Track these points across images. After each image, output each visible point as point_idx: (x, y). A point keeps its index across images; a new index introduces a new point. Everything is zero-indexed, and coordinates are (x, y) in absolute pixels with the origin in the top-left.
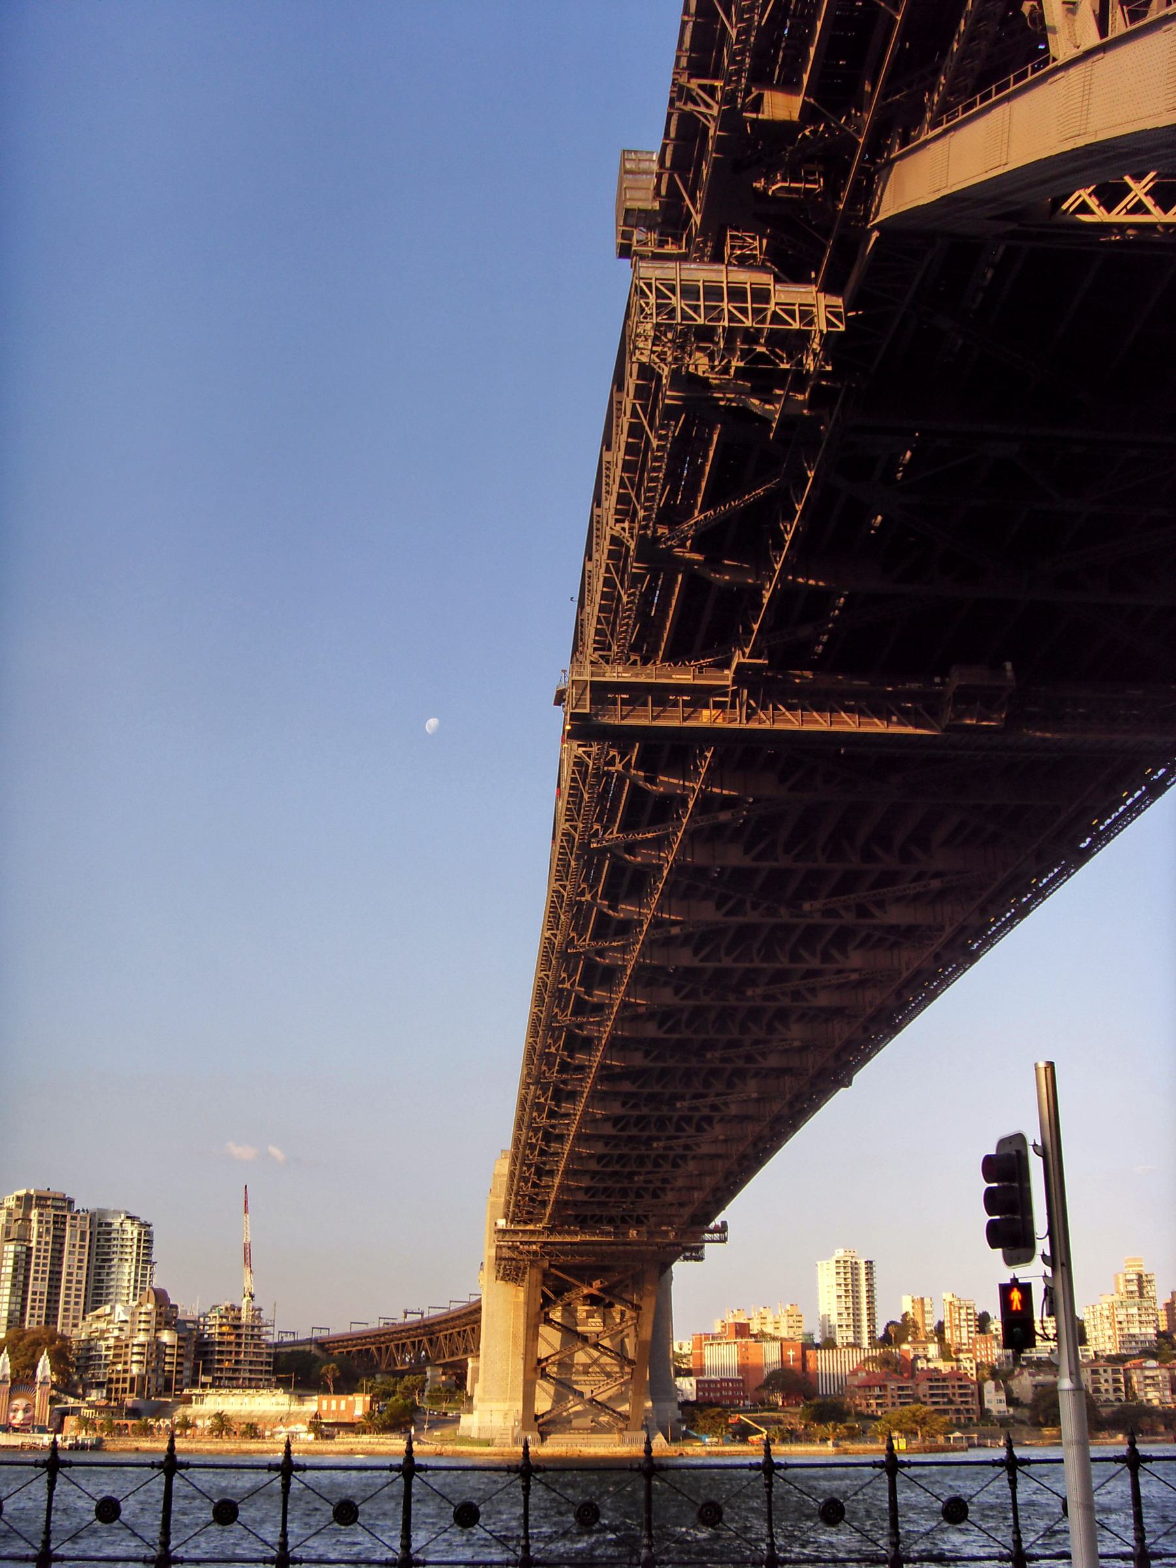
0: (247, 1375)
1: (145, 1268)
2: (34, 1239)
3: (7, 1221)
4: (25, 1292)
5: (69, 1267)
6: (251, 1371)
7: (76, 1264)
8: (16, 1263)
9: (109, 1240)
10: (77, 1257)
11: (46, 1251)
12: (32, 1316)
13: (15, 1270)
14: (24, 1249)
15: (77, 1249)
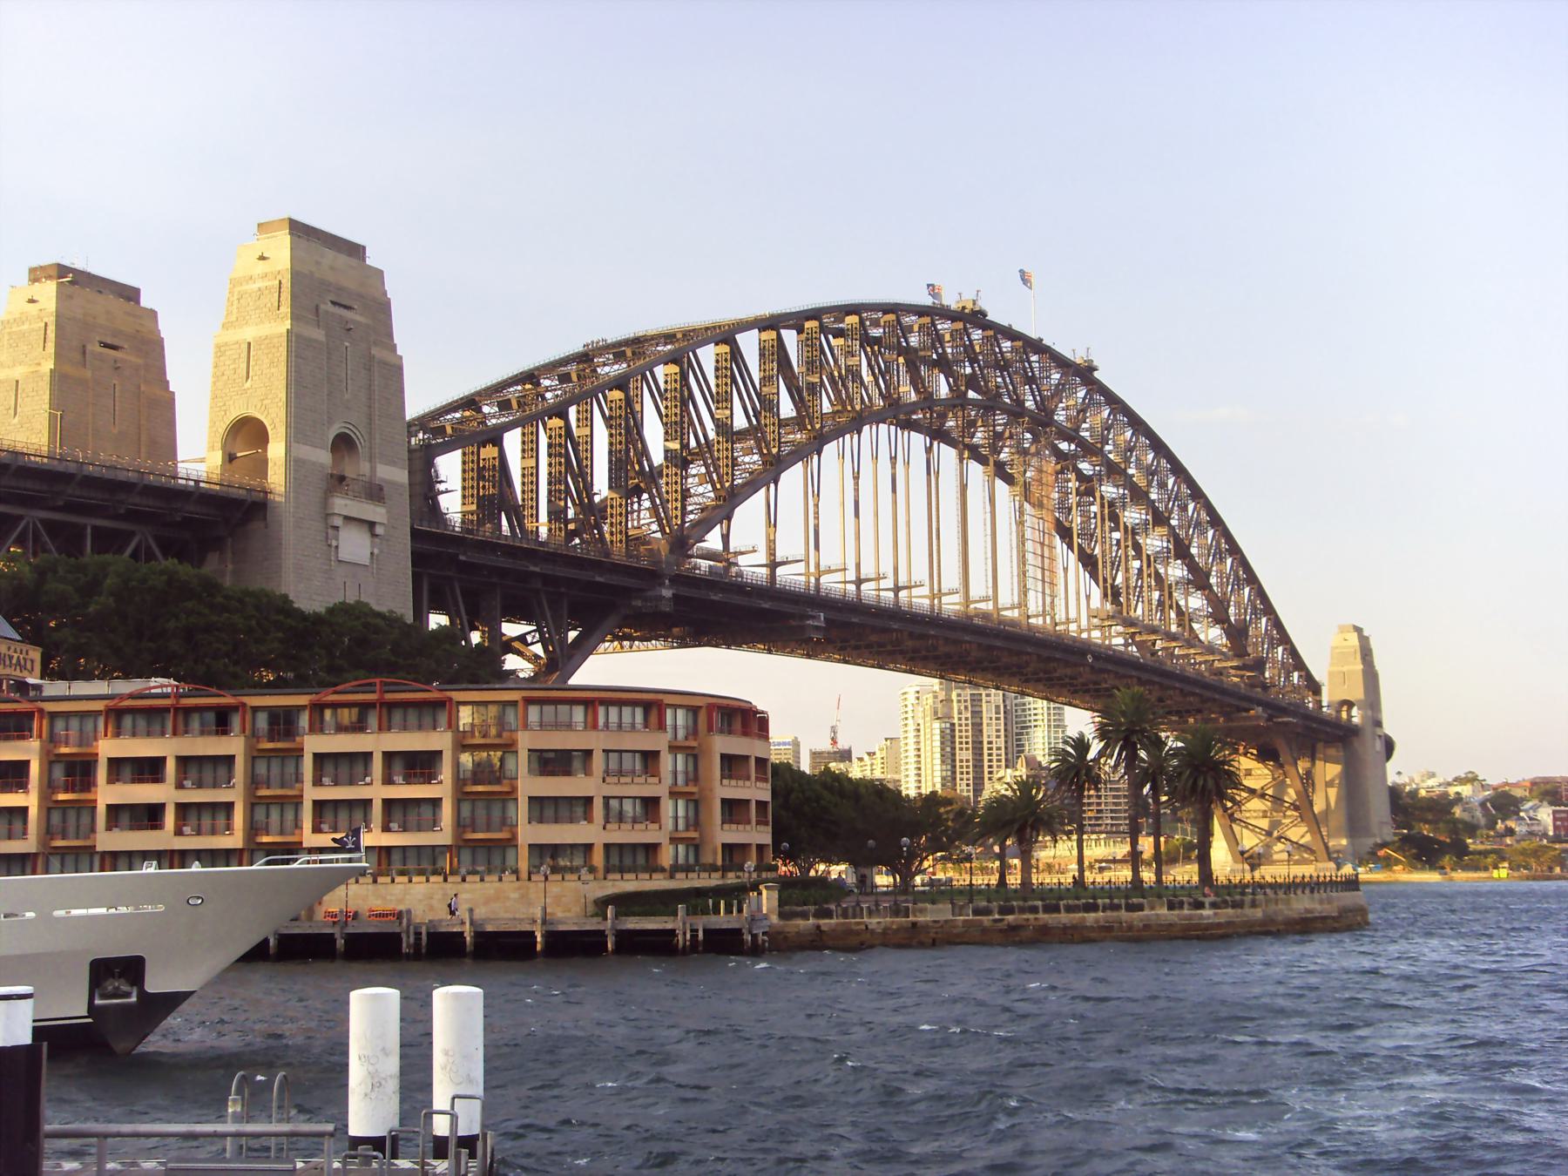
0: (1109, 821)
1: (1056, 732)
2: (956, 715)
3: (934, 703)
4: (954, 761)
5: (989, 736)
6: (1112, 818)
7: (995, 734)
8: (942, 737)
9: (1024, 710)
10: (994, 728)
11: (967, 725)
12: (961, 779)
13: (942, 743)
14: (948, 725)
15: (994, 721)
